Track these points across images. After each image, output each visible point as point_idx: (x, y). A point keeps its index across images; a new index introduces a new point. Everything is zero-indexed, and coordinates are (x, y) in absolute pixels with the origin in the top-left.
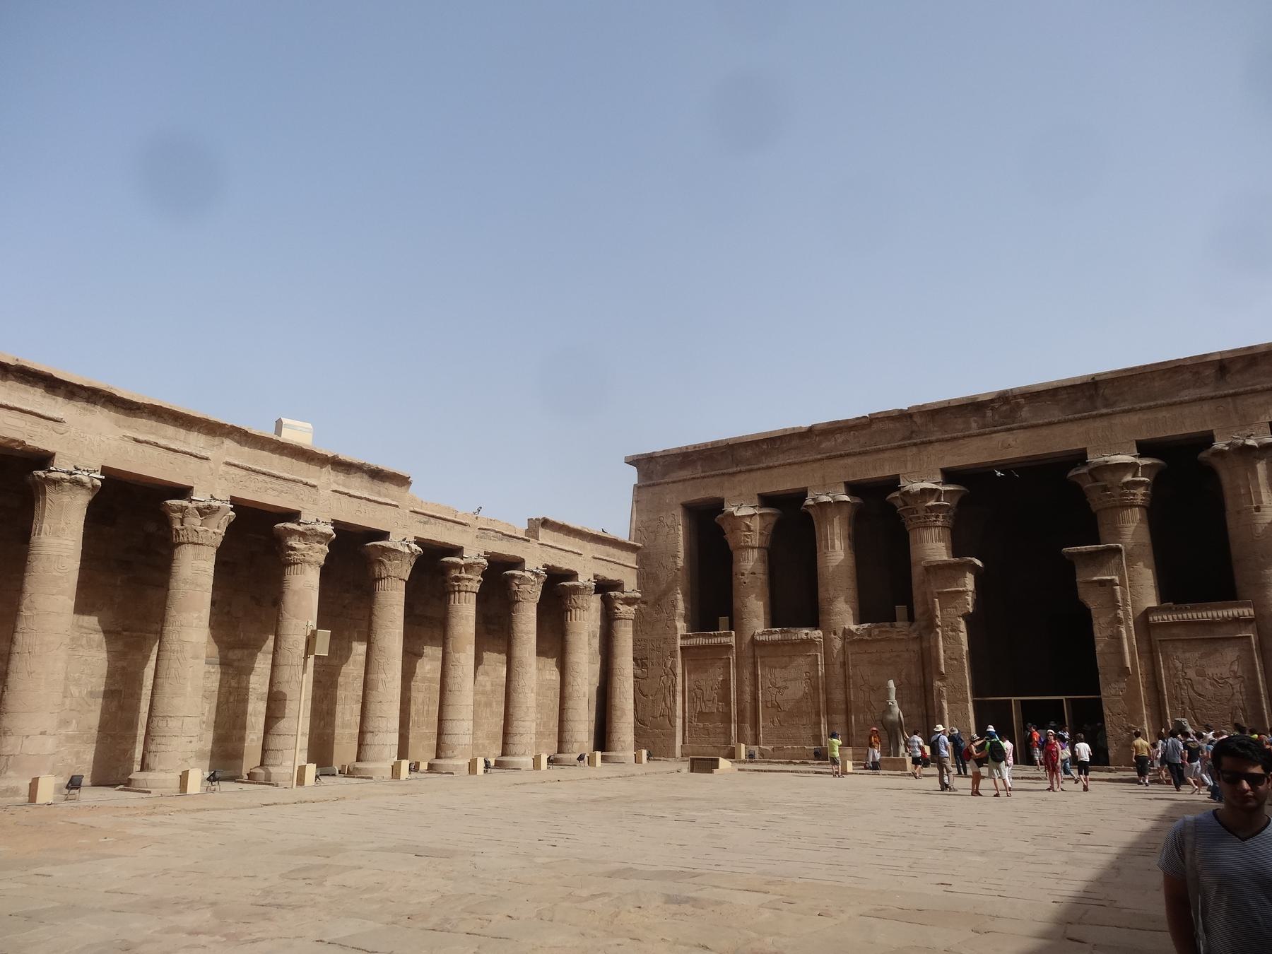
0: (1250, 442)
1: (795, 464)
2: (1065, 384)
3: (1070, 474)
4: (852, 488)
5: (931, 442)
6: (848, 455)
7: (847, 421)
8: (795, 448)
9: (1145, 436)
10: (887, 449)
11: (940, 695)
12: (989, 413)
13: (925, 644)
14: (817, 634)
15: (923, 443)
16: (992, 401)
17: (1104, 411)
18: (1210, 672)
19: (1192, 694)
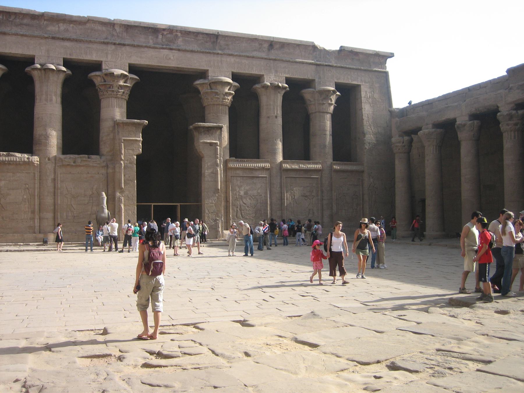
0: (280, 85)
1: (26, 36)
2: (205, 32)
3: (198, 82)
4: (67, 63)
5: (124, 45)
6: (69, 40)
7: (71, 16)
8: (26, 25)
9: (235, 71)
10: (96, 43)
11: (120, 201)
12: (160, 37)
13: (110, 171)
14: (36, 159)
15: (119, 44)
16: (164, 30)
17: (220, 52)
18: (250, 192)
19: (241, 203)
